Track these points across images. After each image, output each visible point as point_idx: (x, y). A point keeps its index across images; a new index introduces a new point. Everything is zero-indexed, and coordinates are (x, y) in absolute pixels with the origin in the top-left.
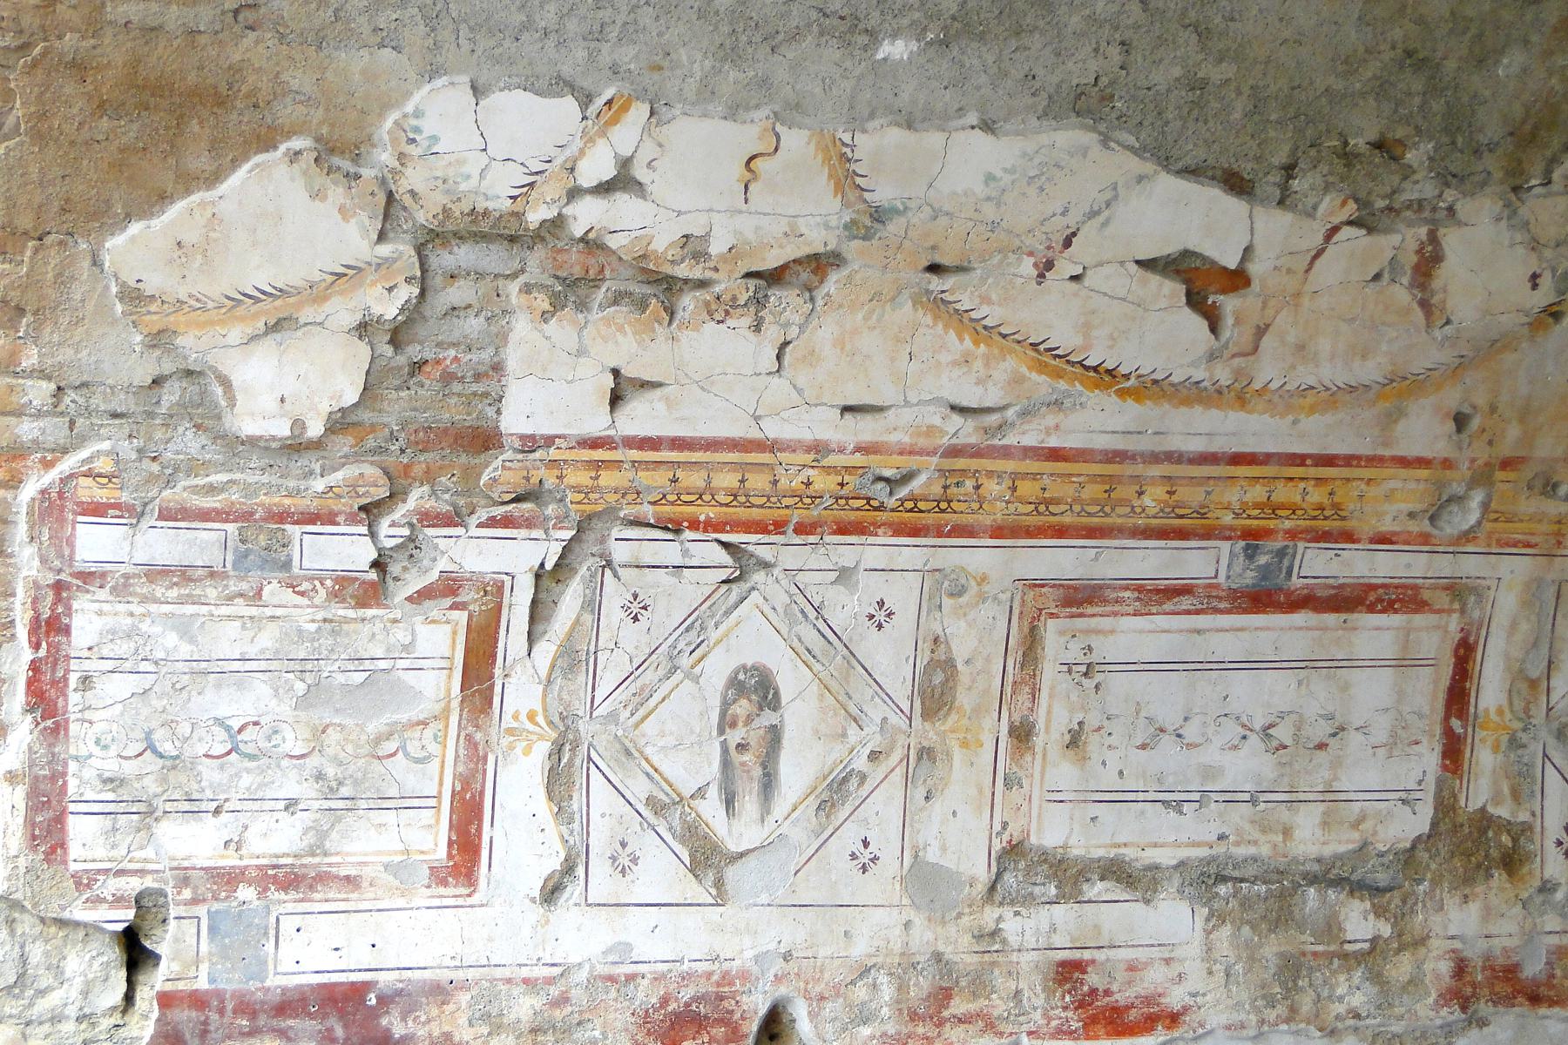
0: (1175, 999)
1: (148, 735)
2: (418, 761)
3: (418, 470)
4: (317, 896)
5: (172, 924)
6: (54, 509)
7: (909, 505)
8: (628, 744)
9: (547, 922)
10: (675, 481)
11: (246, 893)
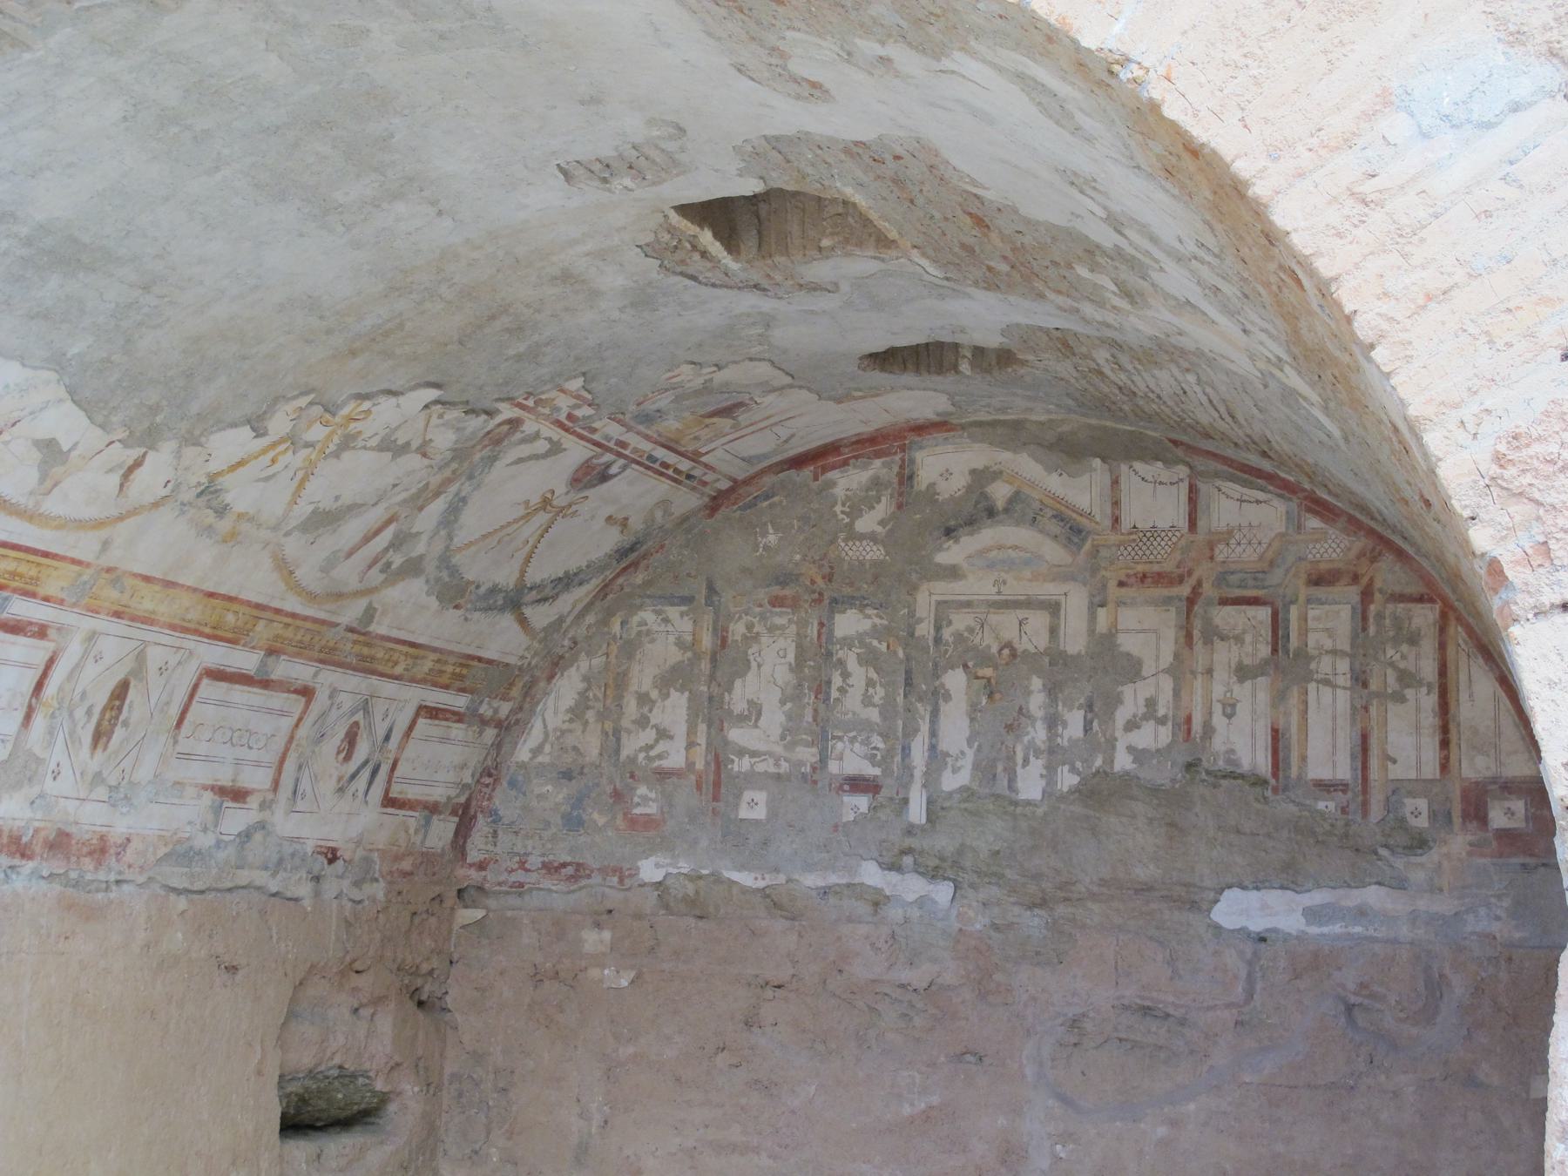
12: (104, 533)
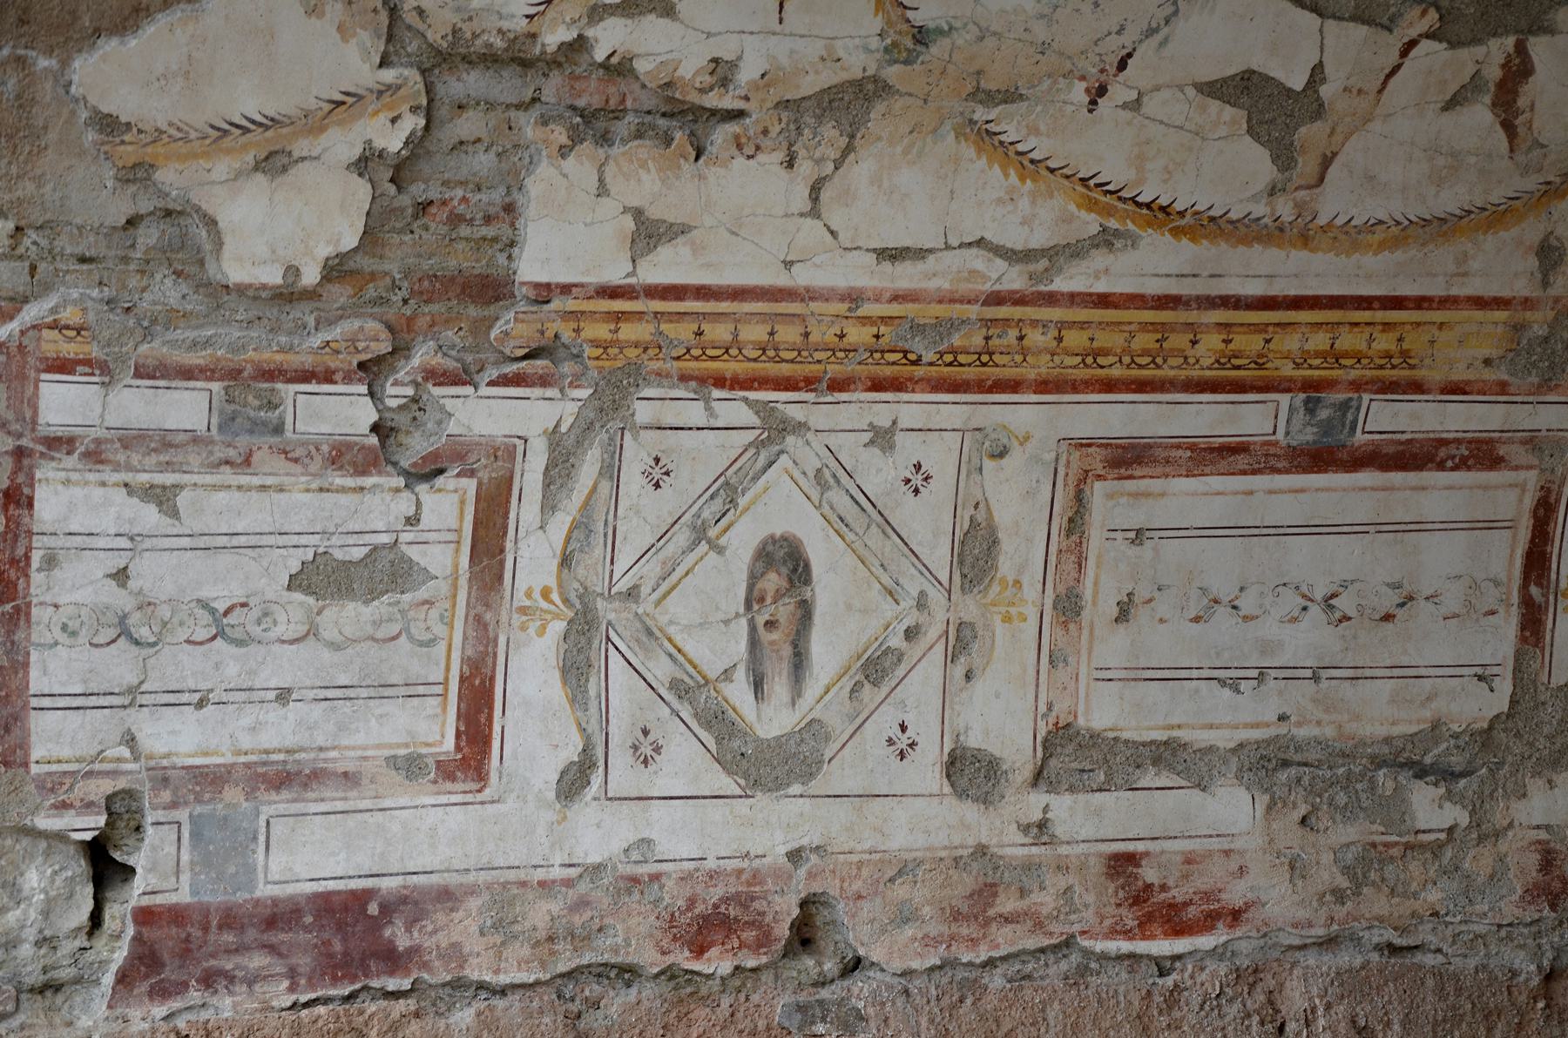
0: (1235, 895)
1: (123, 618)
2: (422, 644)
3: (422, 322)
4: (311, 795)
5: (150, 830)
7: (949, 358)
8: (649, 622)
9: (565, 818)
10: (699, 334)
11: (232, 794)
12: (1532, 230)
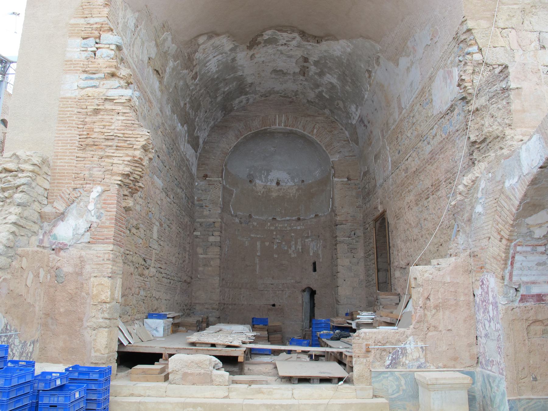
6: (515, 246)
11: (529, 284)
